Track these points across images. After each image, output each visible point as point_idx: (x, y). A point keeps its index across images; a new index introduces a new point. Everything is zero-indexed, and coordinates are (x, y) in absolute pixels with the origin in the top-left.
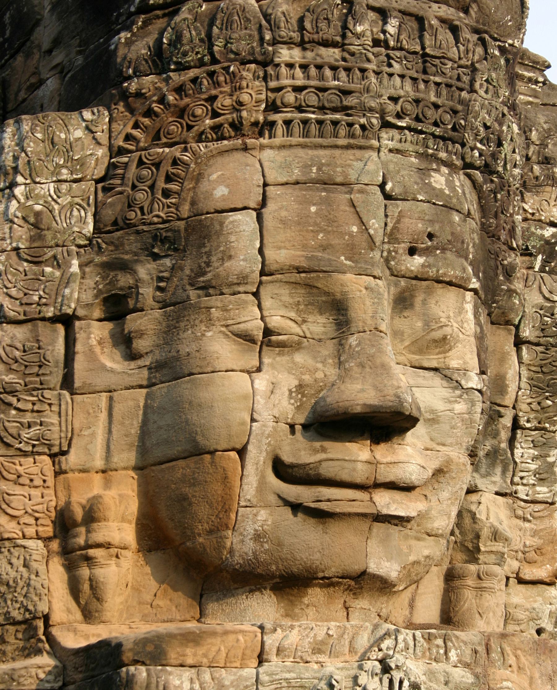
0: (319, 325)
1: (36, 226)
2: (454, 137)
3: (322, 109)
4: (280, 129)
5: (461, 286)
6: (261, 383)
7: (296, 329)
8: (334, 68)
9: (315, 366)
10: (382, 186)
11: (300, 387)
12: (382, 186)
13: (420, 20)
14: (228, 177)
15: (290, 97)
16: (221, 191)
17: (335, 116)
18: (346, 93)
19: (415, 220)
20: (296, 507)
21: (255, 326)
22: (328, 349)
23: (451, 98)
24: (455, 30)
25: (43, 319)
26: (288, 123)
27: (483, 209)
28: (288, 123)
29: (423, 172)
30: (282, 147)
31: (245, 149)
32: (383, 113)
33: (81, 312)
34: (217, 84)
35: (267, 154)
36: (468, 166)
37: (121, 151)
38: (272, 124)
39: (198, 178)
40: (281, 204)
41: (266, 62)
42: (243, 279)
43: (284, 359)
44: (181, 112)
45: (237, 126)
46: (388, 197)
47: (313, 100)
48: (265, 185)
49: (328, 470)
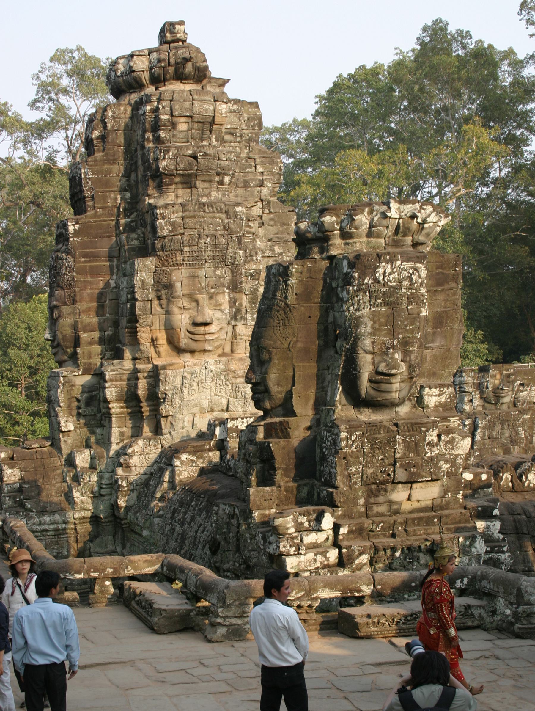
0: (194, 304)
3: (193, 261)
6: (183, 317)
9: (193, 313)
11: (190, 317)
16: (174, 278)
17: (196, 261)
19: (212, 281)
21: (181, 306)
22: (196, 309)
32: (206, 260)
39: (171, 274)
41: (182, 251)
42: (179, 296)
43: (187, 311)
44: (167, 261)
45: (177, 264)
49: (196, 332)
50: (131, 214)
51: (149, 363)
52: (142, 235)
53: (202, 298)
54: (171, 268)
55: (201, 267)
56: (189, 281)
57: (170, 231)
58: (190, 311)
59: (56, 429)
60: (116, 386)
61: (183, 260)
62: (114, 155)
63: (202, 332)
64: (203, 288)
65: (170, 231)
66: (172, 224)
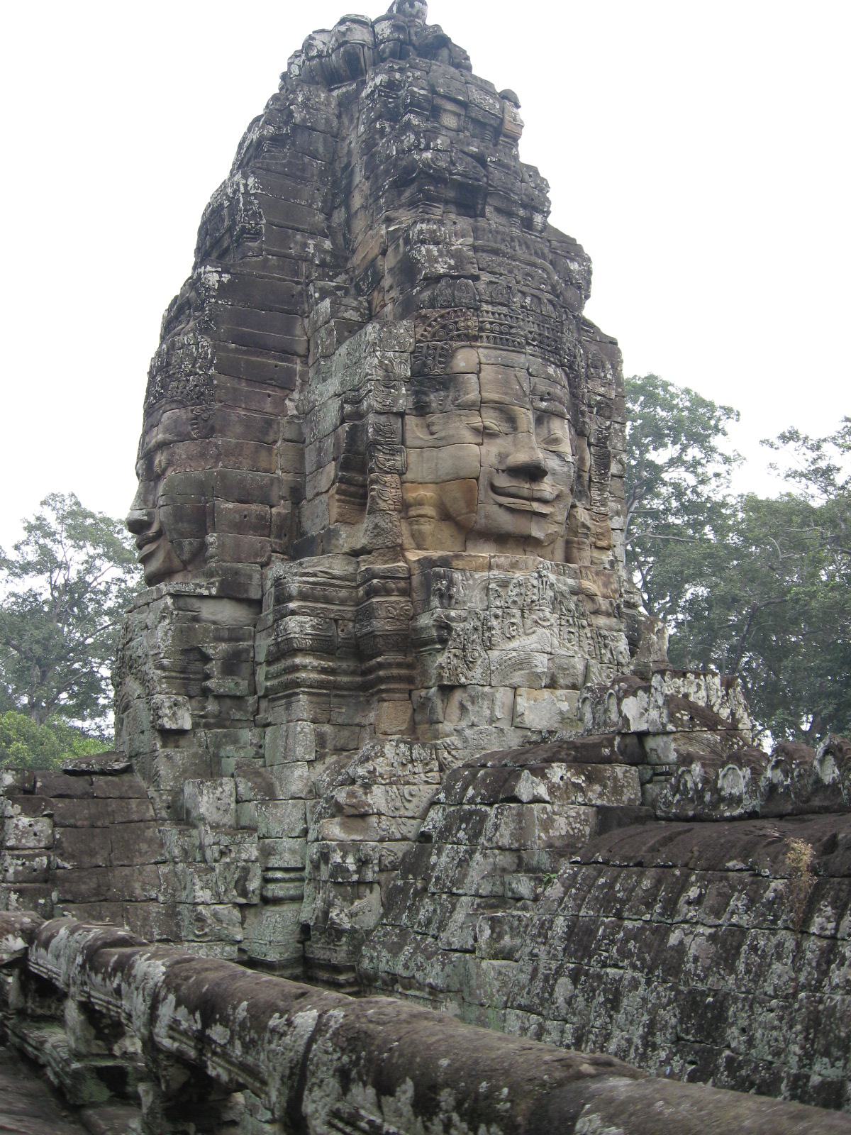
0: (505, 427)
1: (386, 371)
2: (556, 352)
4: (485, 339)
5: (561, 416)
7: (496, 428)
8: (505, 316)
10: (528, 370)
12: (528, 370)
13: (539, 299)
14: (464, 359)
15: (488, 326)
16: (462, 364)
18: (511, 327)
20: (501, 505)
23: (554, 334)
24: (553, 305)
25: (392, 413)
26: (488, 337)
27: (570, 385)
28: (488, 337)
29: (546, 366)
30: (486, 348)
31: (472, 347)
33: (408, 411)
34: (458, 317)
35: (481, 350)
36: (562, 365)
37: (420, 341)
38: (482, 337)
40: (488, 372)
46: (530, 374)
47: (497, 328)
48: (480, 363)
50: (336, 275)
51: (395, 560)
52: (366, 304)
53: (526, 417)
54: (455, 344)
55: (519, 349)
56: (497, 372)
57: (450, 267)
58: (499, 441)
59: (146, 725)
60: (312, 613)
61: (481, 329)
62: (303, 170)
63: (526, 493)
64: (525, 395)
65: (450, 267)
66: (457, 255)
